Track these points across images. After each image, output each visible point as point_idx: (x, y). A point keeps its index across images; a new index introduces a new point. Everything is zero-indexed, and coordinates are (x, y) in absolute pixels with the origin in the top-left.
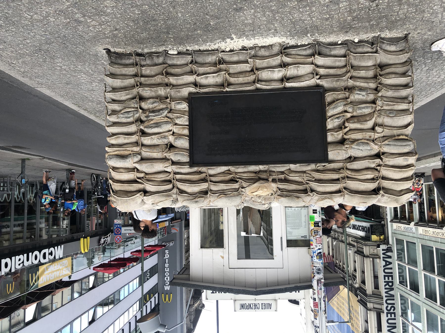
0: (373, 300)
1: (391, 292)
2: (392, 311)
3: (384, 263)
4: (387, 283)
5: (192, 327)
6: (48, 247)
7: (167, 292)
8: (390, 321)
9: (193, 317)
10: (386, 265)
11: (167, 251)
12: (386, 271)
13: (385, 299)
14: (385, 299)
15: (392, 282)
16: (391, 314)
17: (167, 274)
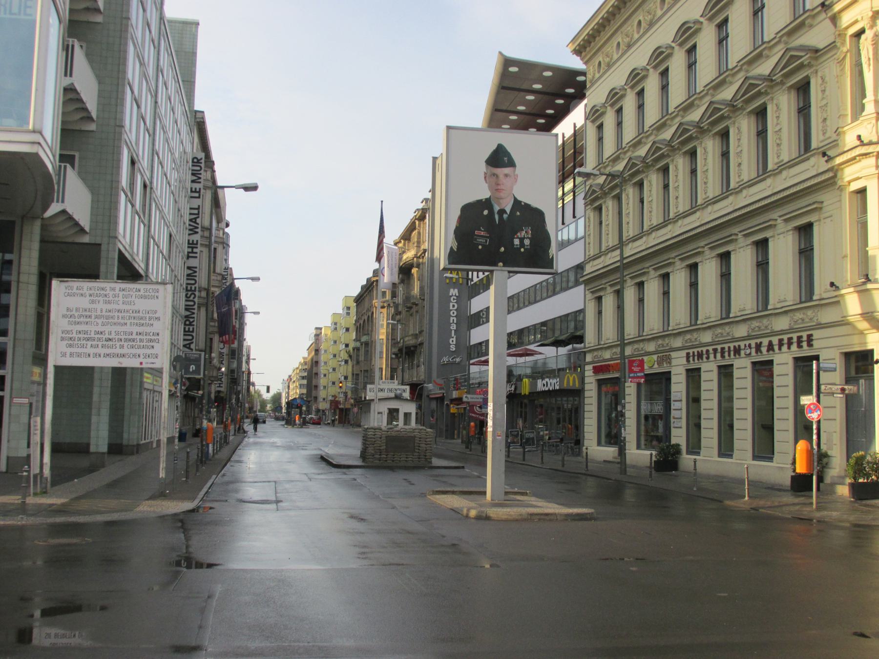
0: (201, 301)
1: (188, 313)
2: (190, 293)
3: (193, 346)
4: (191, 324)
5: (417, 222)
6: (545, 391)
7: (454, 284)
8: (193, 282)
9: (415, 233)
10: (190, 344)
11: (453, 348)
12: (190, 338)
13: (196, 307)
14: (196, 307)
15: (185, 324)
16: (191, 290)
17: (453, 313)
